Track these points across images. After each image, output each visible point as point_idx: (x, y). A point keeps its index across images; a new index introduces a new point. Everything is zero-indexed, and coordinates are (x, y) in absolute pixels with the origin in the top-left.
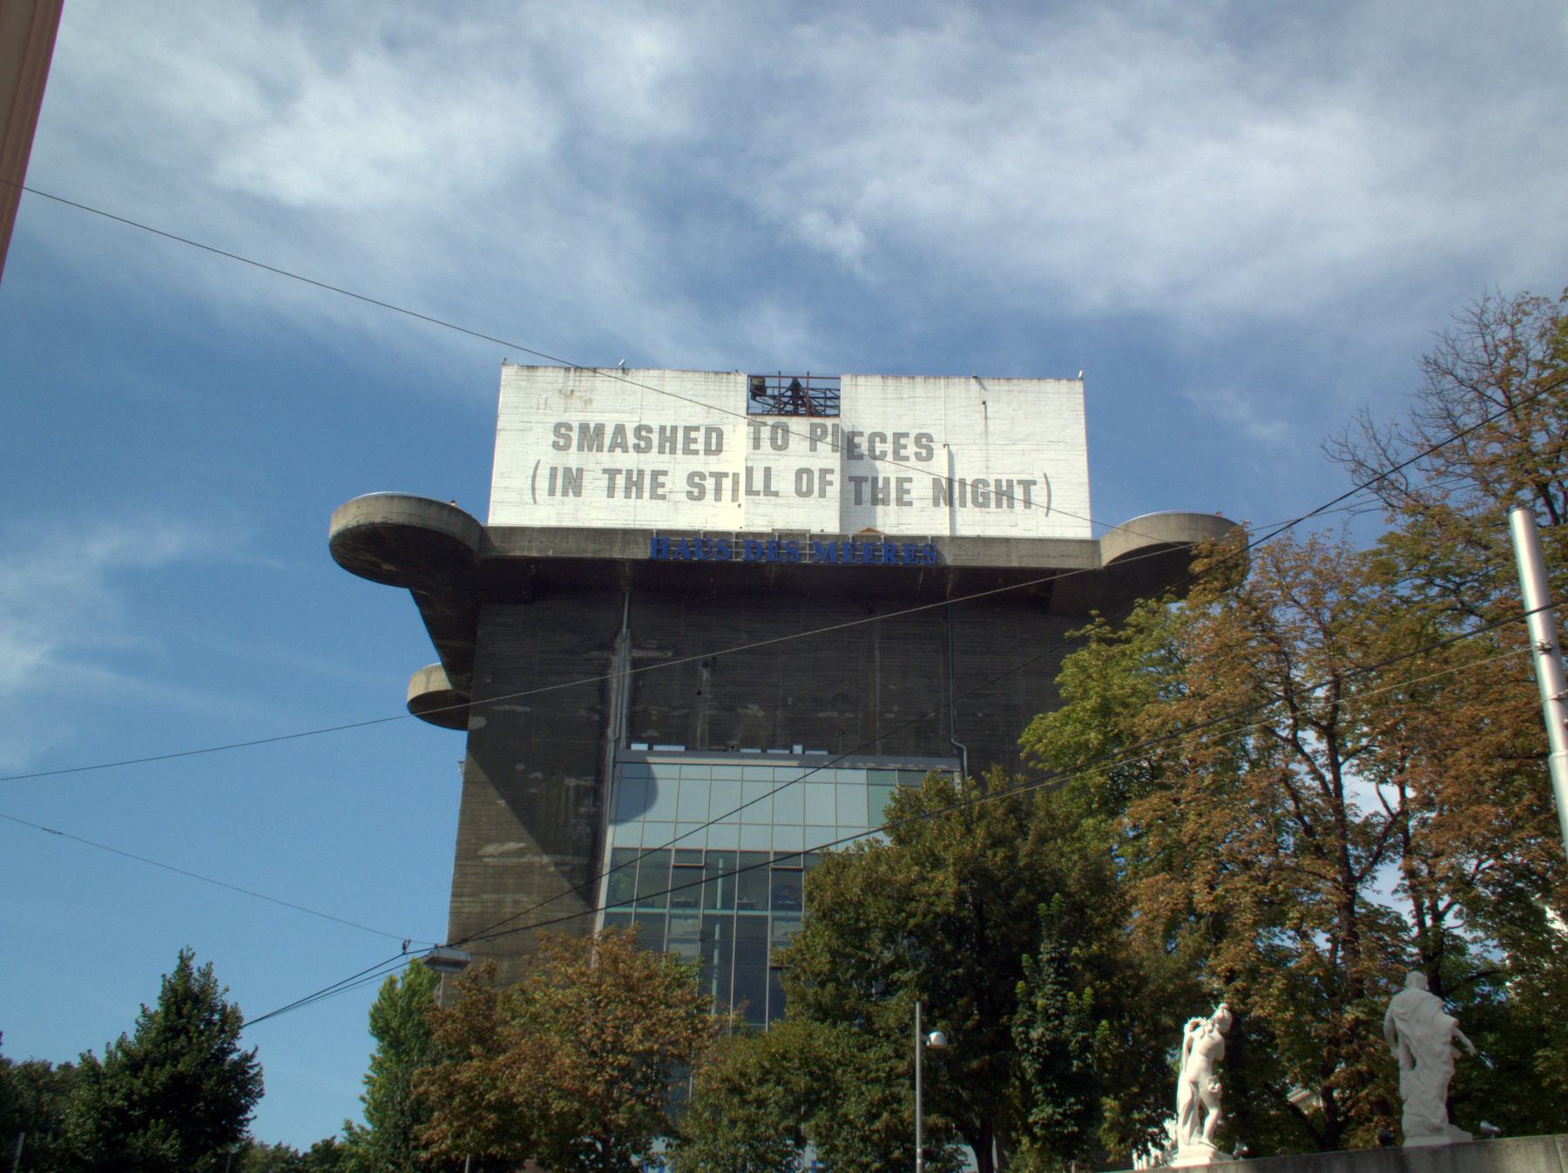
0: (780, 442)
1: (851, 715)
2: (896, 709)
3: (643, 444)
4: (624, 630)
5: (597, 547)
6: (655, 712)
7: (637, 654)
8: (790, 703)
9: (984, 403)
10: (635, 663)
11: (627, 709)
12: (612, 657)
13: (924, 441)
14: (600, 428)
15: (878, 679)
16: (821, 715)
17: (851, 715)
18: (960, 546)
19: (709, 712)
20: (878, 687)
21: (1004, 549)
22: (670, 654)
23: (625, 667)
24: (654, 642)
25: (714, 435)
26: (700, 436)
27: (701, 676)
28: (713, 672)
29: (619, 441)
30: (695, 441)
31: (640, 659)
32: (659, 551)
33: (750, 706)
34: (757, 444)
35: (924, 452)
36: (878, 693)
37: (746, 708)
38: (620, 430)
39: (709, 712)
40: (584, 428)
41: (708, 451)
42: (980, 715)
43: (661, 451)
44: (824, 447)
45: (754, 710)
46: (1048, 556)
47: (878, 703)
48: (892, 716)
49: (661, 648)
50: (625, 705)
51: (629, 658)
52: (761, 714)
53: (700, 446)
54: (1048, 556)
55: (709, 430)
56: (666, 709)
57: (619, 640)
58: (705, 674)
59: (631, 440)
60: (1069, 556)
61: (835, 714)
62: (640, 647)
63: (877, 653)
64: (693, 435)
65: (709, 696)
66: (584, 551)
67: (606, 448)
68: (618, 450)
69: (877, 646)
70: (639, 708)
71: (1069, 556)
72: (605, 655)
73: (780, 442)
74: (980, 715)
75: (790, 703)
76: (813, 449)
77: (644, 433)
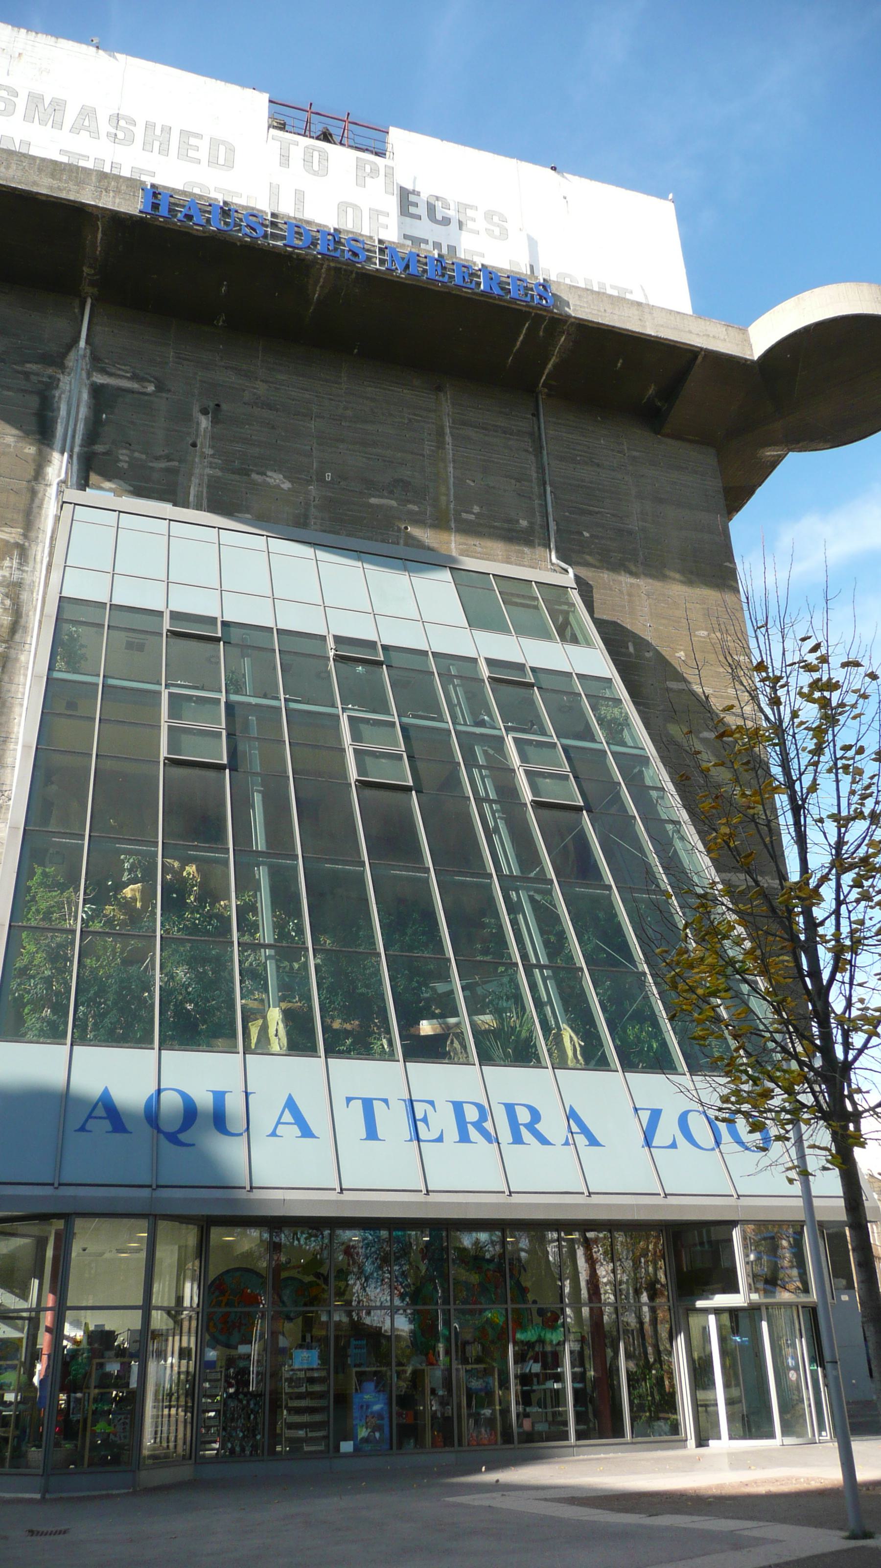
0: (316, 167)
1: (415, 508)
2: (476, 509)
3: (121, 135)
4: (82, 343)
5: (55, 183)
6: (127, 459)
7: (100, 379)
8: (328, 479)
9: (565, 198)
10: (97, 391)
11: (81, 446)
12: (61, 377)
13: (496, 219)
14: (58, 106)
15: (451, 469)
16: (373, 500)
17: (415, 508)
18: (580, 296)
19: (208, 471)
20: (452, 480)
21: (636, 312)
22: (151, 388)
23: (80, 392)
24: (127, 368)
25: (222, 149)
26: (204, 145)
27: (198, 424)
28: (215, 422)
29: (86, 123)
30: (197, 149)
31: (102, 385)
32: (156, 206)
33: (269, 473)
34: (285, 159)
35: (497, 231)
36: (452, 487)
37: (263, 474)
38: (88, 113)
39: (208, 471)
40: (35, 99)
41: (213, 162)
42: (586, 534)
43: (147, 146)
44: (377, 185)
45: (275, 478)
46: (690, 332)
47: (452, 498)
48: (472, 517)
49: (135, 377)
50: (78, 441)
51: (87, 382)
52: (286, 485)
53: (203, 154)
54: (690, 332)
55: (215, 143)
56: (144, 457)
57: (72, 355)
58: (204, 422)
59: (105, 127)
60: (714, 337)
61: (394, 503)
62: (104, 371)
63: (448, 439)
64: (193, 141)
65: (209, 451)
66: (35, 183)
67: (67, 124)
68: (84, 134)
69: (448, 431)
70: (99, 448)
71: (714, 337)
72: (50, 371)
73: (316, 167)
74: (586, 534)
75: (328, 479)
76: (360, 182)
77: (122, 123)
